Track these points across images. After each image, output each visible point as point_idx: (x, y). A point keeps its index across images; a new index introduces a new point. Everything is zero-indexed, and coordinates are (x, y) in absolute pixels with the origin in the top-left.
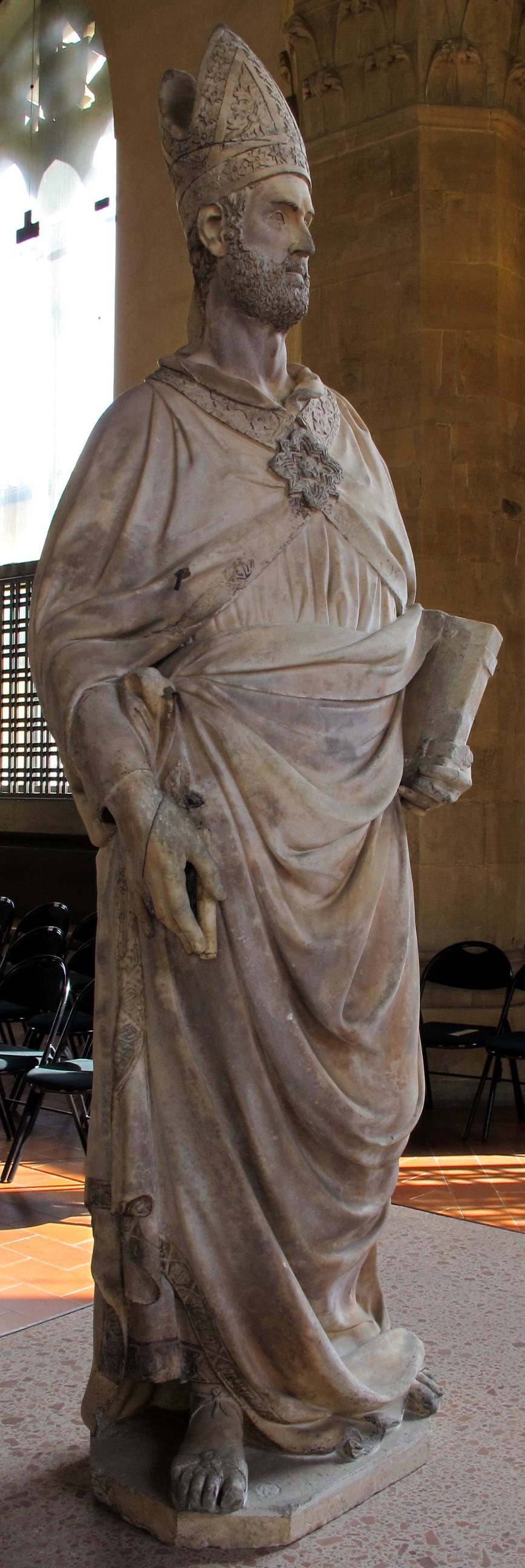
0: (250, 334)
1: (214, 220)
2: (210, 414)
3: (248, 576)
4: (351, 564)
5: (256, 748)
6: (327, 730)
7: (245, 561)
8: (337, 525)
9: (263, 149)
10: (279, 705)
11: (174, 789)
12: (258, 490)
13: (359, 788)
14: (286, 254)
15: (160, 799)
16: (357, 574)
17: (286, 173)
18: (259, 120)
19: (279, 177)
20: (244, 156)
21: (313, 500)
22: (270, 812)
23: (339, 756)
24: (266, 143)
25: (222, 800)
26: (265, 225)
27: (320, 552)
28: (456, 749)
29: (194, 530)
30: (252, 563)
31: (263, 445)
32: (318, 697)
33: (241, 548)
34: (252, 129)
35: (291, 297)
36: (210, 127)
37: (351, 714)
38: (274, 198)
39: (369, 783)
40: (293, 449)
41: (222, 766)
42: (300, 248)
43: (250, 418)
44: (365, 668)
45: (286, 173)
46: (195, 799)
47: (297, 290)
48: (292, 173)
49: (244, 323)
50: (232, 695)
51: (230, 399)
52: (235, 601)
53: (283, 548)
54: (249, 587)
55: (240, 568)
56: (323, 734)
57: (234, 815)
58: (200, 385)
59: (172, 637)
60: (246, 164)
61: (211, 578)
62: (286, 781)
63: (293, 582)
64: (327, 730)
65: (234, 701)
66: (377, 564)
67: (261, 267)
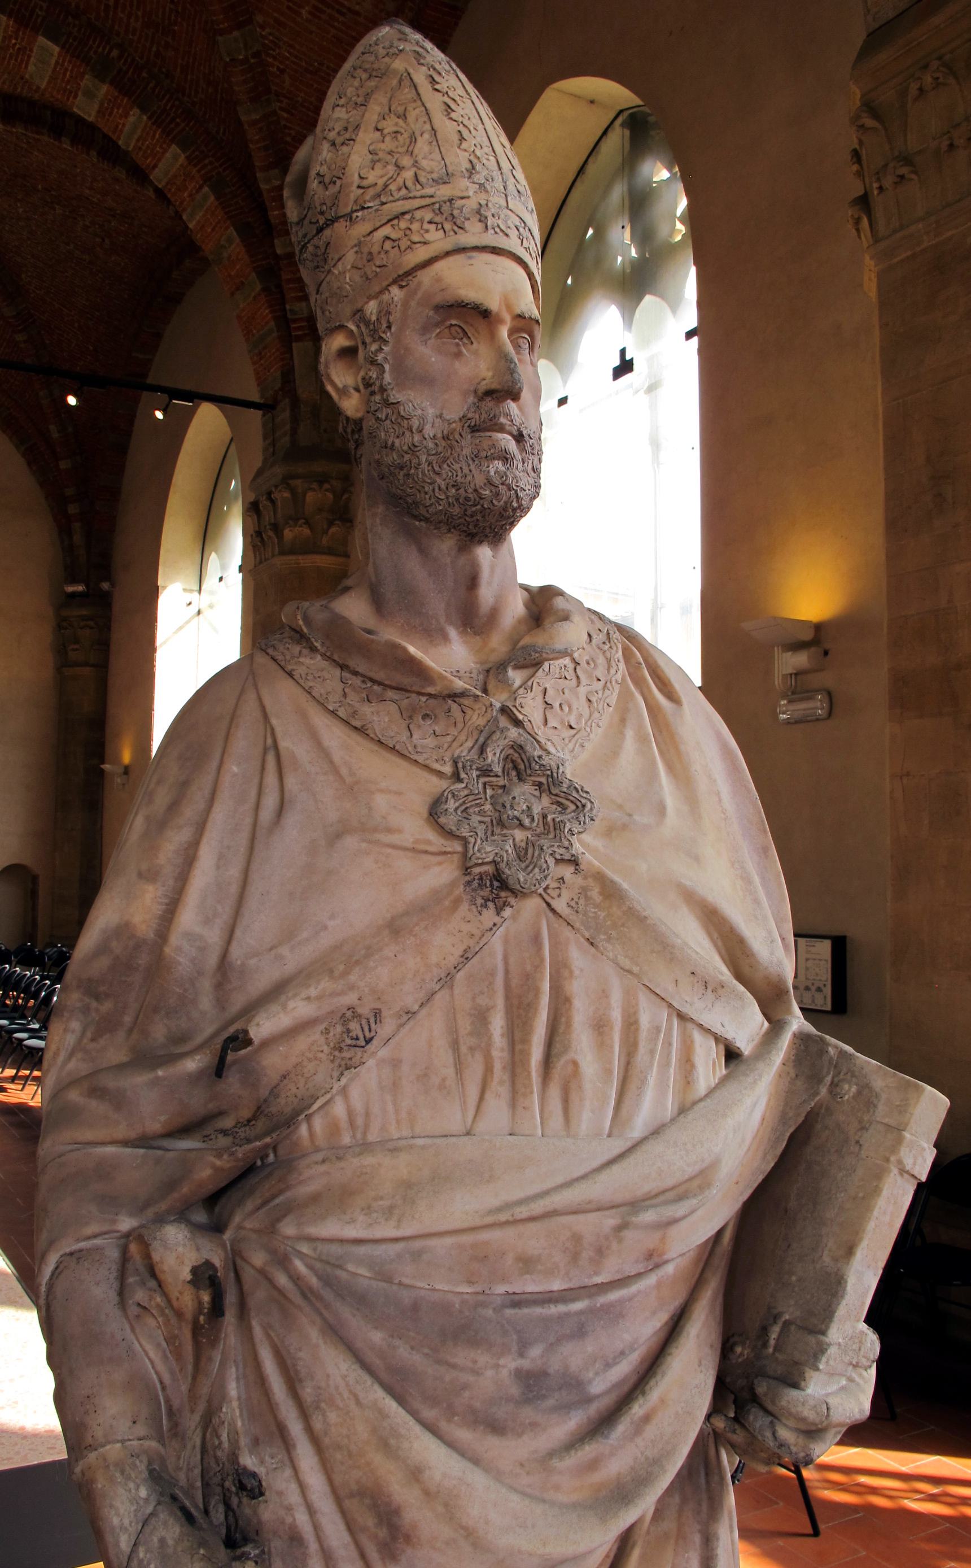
0: (423, 551)
1: (348, 353)
2: (333, 713)
3: (368, 1041)
4: (604, 994)
5: (358, 1402)
6: (521, 1355)
7: (365, 1010)
8: (573, 918)
9: (418, 214)
10: (415, 1307)
11: (219, 1453)
12: (404, 864)
13: (593, 1465)
14: (471, 399)
15: (149, 1509)
16: (616, 1016)
18: (416, 164)
19: (451, 259)
20: (386, 231)
21: (517, 875)
22: (383, 1533)
23: (550, 1402)
24: (428, 201)
25: (294, 1497)
26: (427, 352)
27: (530, 980)
28: (832, 1351)
29: (271, 949)
30: (377, 1014)
31: (426, 767)
32: (501, 1289)
33: (352, 987)
34: (400, 180)
35: (479, 480)
36: (333, 189)
37: (581, 1312)
38: (438, 299)
39: (619, 1454)
40: (486, 772)
41: (295, 1428)
42: (493, 386)
43: (409, 715)
46: (250, 1483)
47: (499, 465)
49: (412, 536)
50: (327, 1281)
51: (372, 680)
52: (344, 1091)
53: (447, 980)
54: (371, 1063)
55: (354, 1026)
56: (510, 1363)
57: (316, 1528)
58: (323, 655)
59: (218, 1163)
60: (388, 245)
61: (302, 1043)
62: (415, 1474)
63: (464, 1049)
64: (521, 1355)
65: (328, 1294)
66: (664, 985)
67: (420, 431)
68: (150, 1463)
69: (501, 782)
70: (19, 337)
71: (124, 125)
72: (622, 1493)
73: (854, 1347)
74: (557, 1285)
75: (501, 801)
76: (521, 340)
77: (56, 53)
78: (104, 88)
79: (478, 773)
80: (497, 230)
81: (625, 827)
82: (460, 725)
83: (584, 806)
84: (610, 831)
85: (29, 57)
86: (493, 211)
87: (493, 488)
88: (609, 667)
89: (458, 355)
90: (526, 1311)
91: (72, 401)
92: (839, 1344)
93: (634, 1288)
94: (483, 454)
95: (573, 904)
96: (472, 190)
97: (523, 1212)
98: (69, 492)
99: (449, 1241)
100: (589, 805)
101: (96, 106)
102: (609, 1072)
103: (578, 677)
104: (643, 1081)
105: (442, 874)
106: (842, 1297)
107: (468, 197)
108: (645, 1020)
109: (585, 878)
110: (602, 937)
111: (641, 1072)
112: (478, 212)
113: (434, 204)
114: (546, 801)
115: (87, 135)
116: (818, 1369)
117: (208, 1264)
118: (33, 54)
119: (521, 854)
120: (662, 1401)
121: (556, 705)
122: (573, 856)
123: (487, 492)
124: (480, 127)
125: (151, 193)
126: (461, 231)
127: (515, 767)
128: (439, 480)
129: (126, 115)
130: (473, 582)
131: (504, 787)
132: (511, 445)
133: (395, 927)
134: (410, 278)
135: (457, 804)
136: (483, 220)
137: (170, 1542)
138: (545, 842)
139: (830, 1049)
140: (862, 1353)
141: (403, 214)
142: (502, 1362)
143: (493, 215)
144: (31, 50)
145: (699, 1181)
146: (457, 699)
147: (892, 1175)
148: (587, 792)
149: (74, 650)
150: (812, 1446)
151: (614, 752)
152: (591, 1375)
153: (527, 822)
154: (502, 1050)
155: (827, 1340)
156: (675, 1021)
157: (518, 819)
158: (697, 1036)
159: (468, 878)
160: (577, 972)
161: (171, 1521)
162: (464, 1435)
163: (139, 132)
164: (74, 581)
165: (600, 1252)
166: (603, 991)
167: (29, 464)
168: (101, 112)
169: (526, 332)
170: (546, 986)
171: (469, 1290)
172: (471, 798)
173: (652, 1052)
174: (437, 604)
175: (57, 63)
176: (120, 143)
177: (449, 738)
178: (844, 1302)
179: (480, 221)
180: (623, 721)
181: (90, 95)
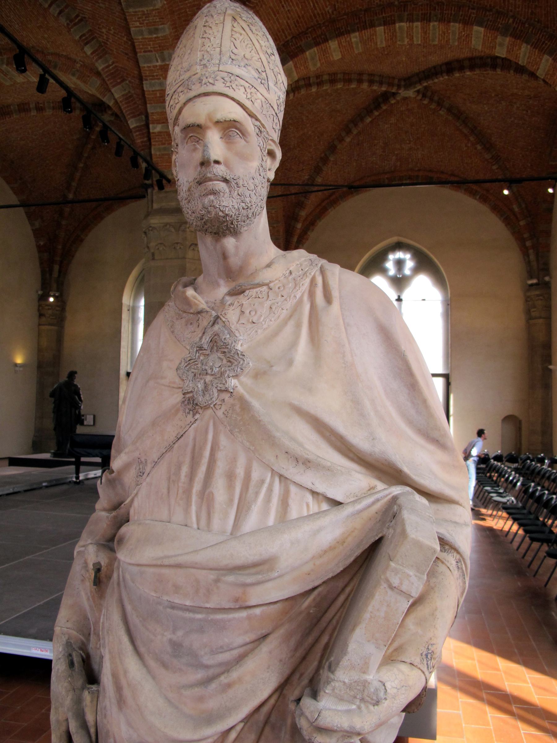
4: (233, 461)
6: (174, 632)
7: (143, 460)
13: (201, 699)
15: (60, 657)
16: (240, 471)
17: (190, 100)
30: (146, 462)
32: (165, 598)
37: (200, 620)
40: (201, 348)
44: (212, 576)
45: (190, 100)
47: (212, 197)
48: (195, 97)
53: (170, 448)
54: (144, 484)
55: (141, 467)
56: (168, 635)
64: (174, 632)
66: (269, 456)
68: (68, 639)
69: (208, 352)
70: (494, 167)
71: (520, 53)
72: (209, 719)
73: (359, 688)
74: (188, 603)
76: (231, 132)
77: (483, 32)
78: (508, 39)
79: (198, 349)
80: (208, 84)
81: (265, 373)
84: (257, 375)
85: (471, 37)
86: (207, 75)
88: (295, 288)
89: (195, 149)
90: (175, 612)
91: (506, 192)
92: (344, 682)
93: (231, 616)
94: (202, 194)
95: (226, 413)
96: (198, 69)
97: (166, 562)
98: (526, 235)
99: (152, 570)
100: (242, 362)
101: (505, 50)
102: (231, 500)
104: (249, 508)
105: (178, 397)
106: (345, 654)
107: (197, 73)
108: (255, 475)
109: (234, 400)
110: (236, 430)
111: (249, 503)
114: (225, 361)
115: (506, 64)
116: (325, 692)
117: (99, 563)
118: (473, 36)
119: (206, 388)
120: (240, 680)
124: (219, 35)
125: (542, 82)
127: (216, 346)
129: (520, 49)
130: (225, 256)
131: (208, 355)
132: (222, 186)
133: (154, 424)
135: (186, 364)
136: (200, 81)
137: (60, 671)
138: (216, 381)
139: (395, 506)
140: (366, 693)
141: (174, 92)
142: (165, 634)
143: (207, 78)
144: (472, 34)
145: (263, 566)
147: (382, 587)
149: (533, 311)
150: (315, 735)
151: (276, 333)
152: (203, 653)
153: (209, 371)
154: (184, 483)
155: (332, 676)
156: (277, 480)
158: (293, 489)
159: (183, 400)
160: (222, 448)
161: (63, 663)
162: (152, 664)
163: (527, 55)
164: (531, 277)
165: (209, 592)
166: (235, 458)
167: (506, 225)
168: (508, 51)
169: (233, 128)
170: (207, 453)
171: (155, 595)
172: (192, 361)
173: (257, 494)
175: (484, 36)
176: (520, 63)
177: (195, 333)
178: (346, 658)
180: (291, 317)
181: (501, 45)
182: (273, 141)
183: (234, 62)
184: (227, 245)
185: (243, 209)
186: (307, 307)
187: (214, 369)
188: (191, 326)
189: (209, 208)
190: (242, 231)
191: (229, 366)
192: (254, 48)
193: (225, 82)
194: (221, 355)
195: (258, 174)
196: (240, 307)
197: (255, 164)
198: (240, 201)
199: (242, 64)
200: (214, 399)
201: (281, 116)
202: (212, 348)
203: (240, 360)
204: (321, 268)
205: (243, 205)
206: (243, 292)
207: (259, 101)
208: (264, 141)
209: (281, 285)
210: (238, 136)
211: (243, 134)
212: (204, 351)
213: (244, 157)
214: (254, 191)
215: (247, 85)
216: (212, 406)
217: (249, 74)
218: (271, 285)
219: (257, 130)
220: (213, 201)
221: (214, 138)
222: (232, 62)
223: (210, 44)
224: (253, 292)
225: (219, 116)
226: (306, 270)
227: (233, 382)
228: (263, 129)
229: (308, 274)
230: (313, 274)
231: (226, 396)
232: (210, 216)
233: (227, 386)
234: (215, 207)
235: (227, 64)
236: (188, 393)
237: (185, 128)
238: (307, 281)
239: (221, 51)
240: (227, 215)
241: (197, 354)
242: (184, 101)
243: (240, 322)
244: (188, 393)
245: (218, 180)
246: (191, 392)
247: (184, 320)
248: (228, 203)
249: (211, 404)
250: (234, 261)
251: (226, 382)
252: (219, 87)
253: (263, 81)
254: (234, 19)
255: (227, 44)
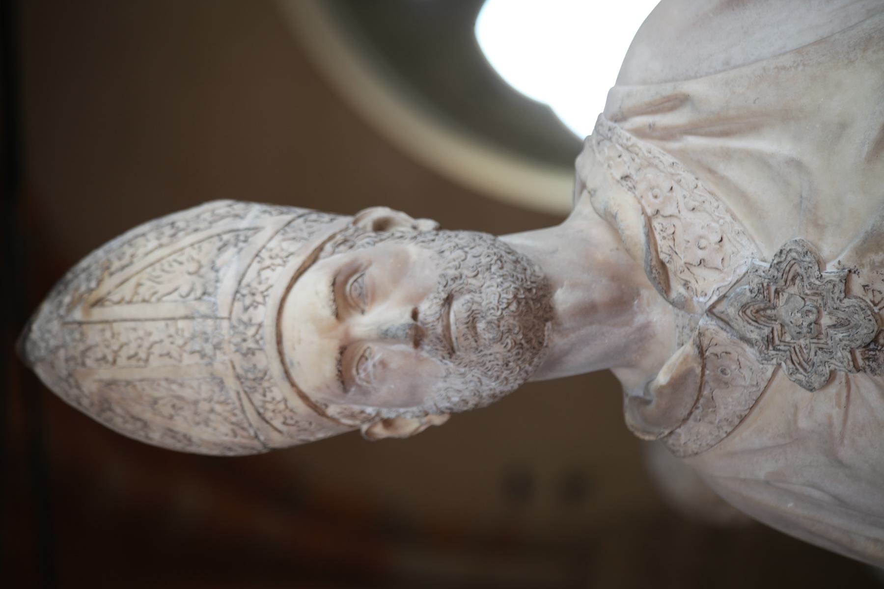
0: (566, 353)
2: (728, 434)
17: (287, 374)
20: (277, 423)
31: (770, 381)
40: (769, 340)
45: (287, 374)
47: (481, 325)
48: (283, 362)
60: (289, 421)
69: (777, 327)
75: (795, 334)
79: (771, 348)
80: (258, 337)
82: (728, 350)
83: (794, 259)
87: (505, 336)
88: (656, 167)
94: (474, 344)
100: (794, 254)
103: (671, 216)
109: (863, 265)
112: (245, 355)
113: (245, 392)
114: (793, 290)
121: (701, 254)
122: (841, 281)
123: (509, 341)
126: (268, 373)
127: (764, 309)
128: (504, 375)
131: (782, 325)
132: (458, 307)
134: (318, 405)
135: (801, 370)
136: (251, 352)
143: (244, 340)
146: (704, 349)
148: (781, 252)
153: (812, 317)
157: (811, 324)
159: (868, 370)
174: (614, 335)
177: (742, 359)
179: (253, 354)
180: (711, 171)
182: (355, 223)
183: (210, 290)
184: (569, 305)
185: (502, 268)
186: (694, 142)
187: (806, 308)
188: (728, 371)
189: (502, 329)
190: (542, 275)
191: (802, 280)
192: (171, 258)
193: (255, 305)
194: (783, 298)
195: (432, 244)
196: (693, 269)
197: (413, 249)
198: (487, 274)
199: (212, 275)
200: (863, 305)
201: (300, 211)
202: (770, 318)
203: (789, 259)
204: (616, 121)
205: (494, 268)
206: (663, 264)
207: (285, 245)
208: (361, 236)
209: (650, 194)
210: (360, 280)
211: (354, 270)
212: (776, 333)
213: (401, 268)
214: (467, 249)
215: (255, 266)
216: (876, 309)
217: (230, 266)
218: (650, 211)
219: (342, 248)
220: (489, 323)
221: (363, 324)
222: (209, 294)
223: (167, 342)
224: (663, 245)
225: (326, 312)
226: (619, 148)
227: (831, 269)
228: (339, 238)
229: (629, 143)
230: (628, 135)
231: (857, 283)
232: (517, 329)
233: (838, 280)
234: (501, 317)
235: (215, 304)
236: (854, 360)
237: (343, 382)
238: (643, 145)
239: (186, 318)
240: (515, 297)
241: (782, 347)
242: (287, 385)
243: (720, 267)
244: (854, 360)
245: (448, 313)
246: (852, 352)
247: (717, 393)
248: (492, 294)
249: (872, 311)
250: (600, 292)
251: (830, 282)
252: (264, 314)
253: (242, 238)
254: (99, 302)
255: (166, 308)
